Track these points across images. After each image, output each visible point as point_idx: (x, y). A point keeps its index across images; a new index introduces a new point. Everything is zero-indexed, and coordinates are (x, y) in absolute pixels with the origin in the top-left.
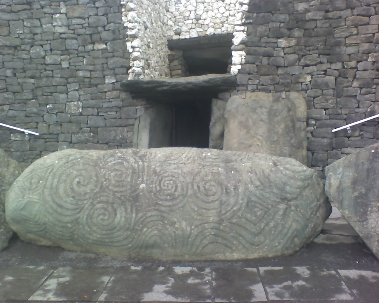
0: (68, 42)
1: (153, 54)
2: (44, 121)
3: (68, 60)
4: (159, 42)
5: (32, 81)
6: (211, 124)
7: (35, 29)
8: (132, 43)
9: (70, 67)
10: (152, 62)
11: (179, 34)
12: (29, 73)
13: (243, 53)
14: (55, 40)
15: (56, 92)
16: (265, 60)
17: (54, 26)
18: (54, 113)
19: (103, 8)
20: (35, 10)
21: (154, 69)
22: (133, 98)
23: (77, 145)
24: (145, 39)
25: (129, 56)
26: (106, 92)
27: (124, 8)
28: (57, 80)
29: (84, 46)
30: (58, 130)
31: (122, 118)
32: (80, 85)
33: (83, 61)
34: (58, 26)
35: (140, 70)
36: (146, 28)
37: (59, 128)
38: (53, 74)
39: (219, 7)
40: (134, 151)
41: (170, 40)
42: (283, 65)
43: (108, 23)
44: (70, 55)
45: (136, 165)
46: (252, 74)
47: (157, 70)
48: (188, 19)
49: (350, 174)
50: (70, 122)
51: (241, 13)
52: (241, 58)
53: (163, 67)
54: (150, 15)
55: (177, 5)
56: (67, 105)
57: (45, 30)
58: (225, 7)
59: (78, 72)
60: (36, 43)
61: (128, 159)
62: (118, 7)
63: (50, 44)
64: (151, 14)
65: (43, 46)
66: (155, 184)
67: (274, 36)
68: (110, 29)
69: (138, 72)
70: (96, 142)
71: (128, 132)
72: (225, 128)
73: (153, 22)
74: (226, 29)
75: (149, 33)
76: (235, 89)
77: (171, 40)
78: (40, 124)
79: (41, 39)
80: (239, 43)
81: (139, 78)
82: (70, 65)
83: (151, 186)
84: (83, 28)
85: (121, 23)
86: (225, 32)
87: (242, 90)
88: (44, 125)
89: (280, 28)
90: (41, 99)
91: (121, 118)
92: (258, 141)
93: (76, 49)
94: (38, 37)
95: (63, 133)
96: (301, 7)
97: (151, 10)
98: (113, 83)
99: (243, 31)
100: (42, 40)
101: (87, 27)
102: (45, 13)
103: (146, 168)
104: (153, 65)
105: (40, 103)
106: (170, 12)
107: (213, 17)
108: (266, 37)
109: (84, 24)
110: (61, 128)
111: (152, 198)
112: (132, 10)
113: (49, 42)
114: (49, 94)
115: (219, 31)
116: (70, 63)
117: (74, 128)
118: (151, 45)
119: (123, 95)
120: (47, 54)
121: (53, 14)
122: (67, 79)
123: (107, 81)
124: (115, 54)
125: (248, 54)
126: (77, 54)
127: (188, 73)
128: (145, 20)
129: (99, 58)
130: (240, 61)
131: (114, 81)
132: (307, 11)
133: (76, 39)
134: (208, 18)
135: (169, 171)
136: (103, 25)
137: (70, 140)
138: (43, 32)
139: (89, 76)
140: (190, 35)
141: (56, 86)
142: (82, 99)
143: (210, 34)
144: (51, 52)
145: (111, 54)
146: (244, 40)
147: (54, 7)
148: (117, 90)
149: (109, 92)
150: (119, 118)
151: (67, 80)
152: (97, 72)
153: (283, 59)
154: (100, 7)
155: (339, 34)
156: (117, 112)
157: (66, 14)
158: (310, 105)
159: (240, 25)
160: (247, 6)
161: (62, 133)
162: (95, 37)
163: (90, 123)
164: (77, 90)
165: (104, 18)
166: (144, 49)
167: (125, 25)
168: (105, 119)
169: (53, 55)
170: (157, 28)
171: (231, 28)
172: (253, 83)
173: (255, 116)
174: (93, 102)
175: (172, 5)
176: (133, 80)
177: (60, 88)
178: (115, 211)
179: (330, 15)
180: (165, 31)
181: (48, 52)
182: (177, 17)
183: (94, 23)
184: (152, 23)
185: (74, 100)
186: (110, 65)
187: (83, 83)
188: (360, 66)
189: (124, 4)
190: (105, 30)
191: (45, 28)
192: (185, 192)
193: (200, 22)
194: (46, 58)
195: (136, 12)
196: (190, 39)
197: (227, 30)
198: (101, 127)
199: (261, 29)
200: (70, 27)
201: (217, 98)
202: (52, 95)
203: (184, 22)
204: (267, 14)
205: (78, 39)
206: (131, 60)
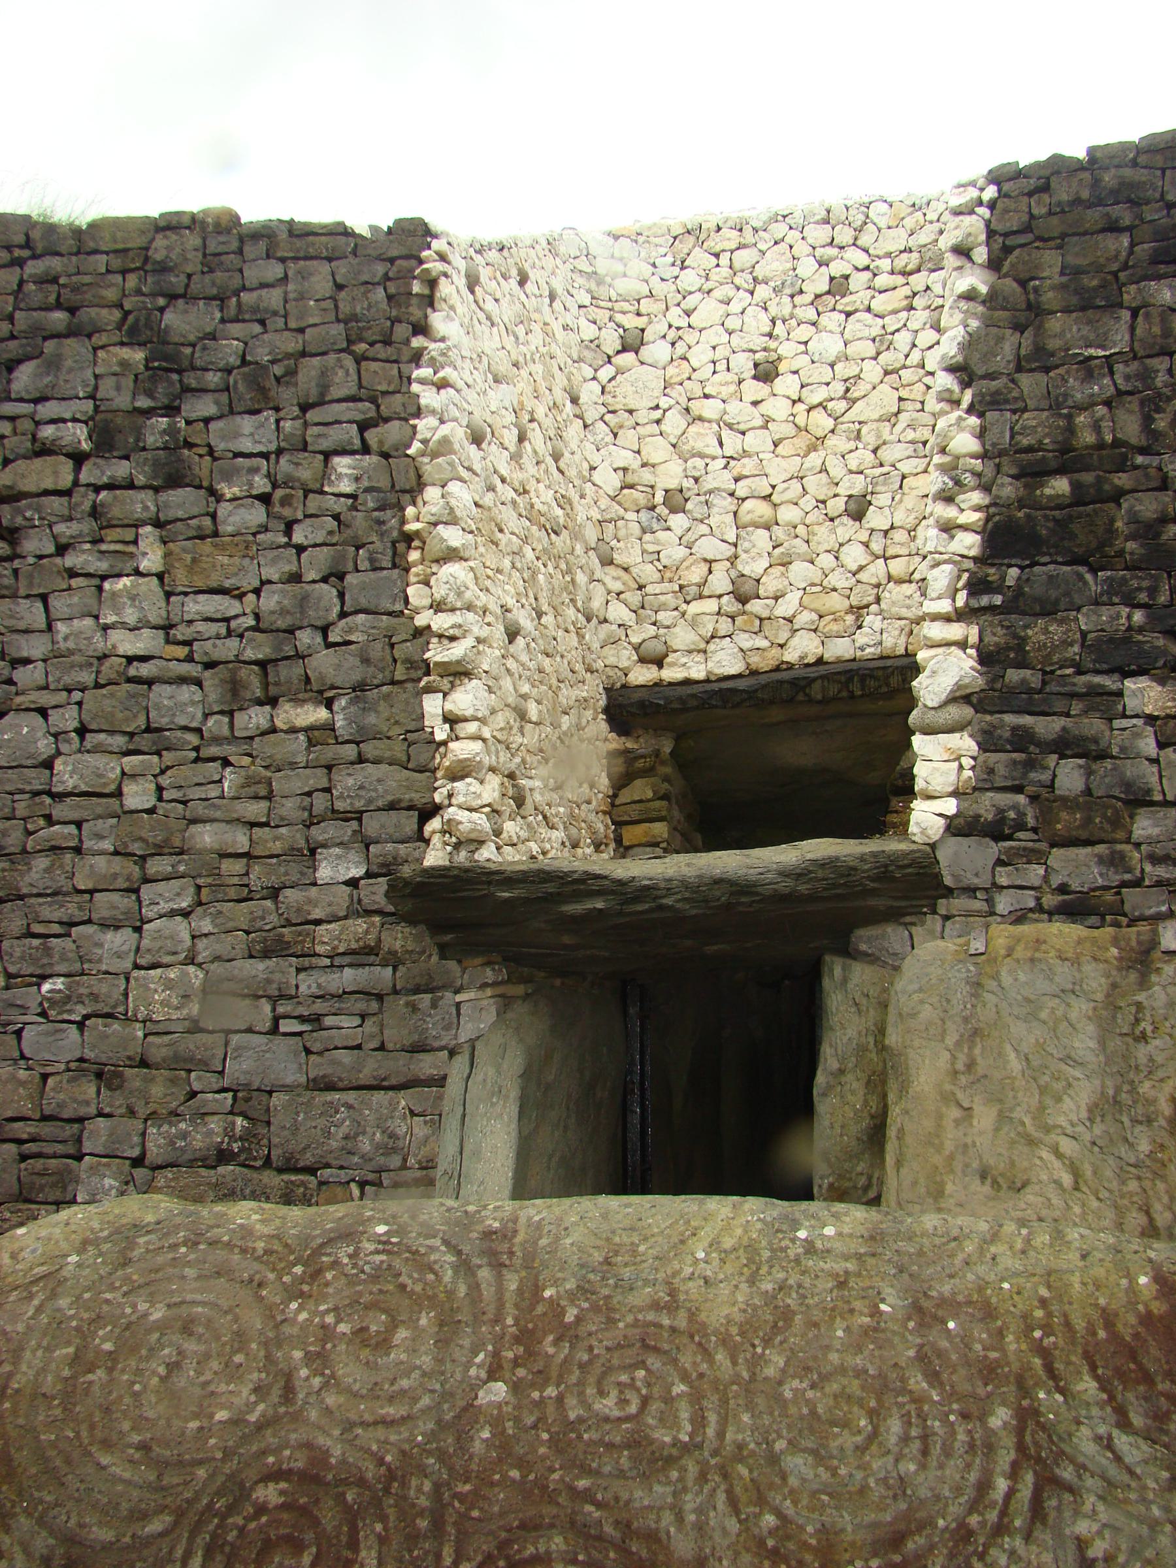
0: (162, 694)
1: (541, 751)
2: (23, 1057)
3: (155, 776)
4: (568, 695)
6: (821, 1079)
7: (21, 639)
8: (449, 697)
9: (162, 807)
10: (534, 785)
11: (659, 663)
13: (966, 743)
14: (103, 686)
15: (89, 921)
16: (1070, 777)
17: (106, 628)
18: (73, 1017)
19: (325, 549)
20: (31, 560)
21: (545, 817)
22: (444, 951)
23: (169, 1173)
24: (507, 683)
25: (434, 757)
26: (318, 922)
27: (416, 548)
29: (231, 714)
30: (88, 1103)
31: (390, 1046)
32: (199, 888)
33: (220, 781)
34: (123, 625)
35: (481, 820)
36: (512, 634)
37: (93, 1089)
38: (81, 841)
39: (841, 545)
40: (449, 1210)
41: (618, 685)
42: (1158, 797)
43: (343, 615)
44: (164, 753)
45: (462, 1290)
46: (1010, 838)
47: (556, 820)
48: (701, 597)
50: (144, 1063)
51: (947, 568)
52: (956, 764)
53: (584, 807)
54: (530, 580)
55: (647, 537)
56: (132, 981)
57: (62, 645)
58: (866, 545)
59: (195, 829)
60: (19, 700)
61: (422, 1250)
62: (394, 543)
63: (80, 704)
64: (534, 574)
65: (50, 712)
66: (558, 1386)
67: (1105, 666)
68: (353, 638)
69: (473, 830)
70: (259, 1163)
71: (413, 1114)
72: (891, 1097)
73: (545, 608)
74: (876, 637)
75: (524, 658)
76: (934, 912)
77: (624, 686)
79: (42, 682)
80: (943, 697)
81: (476, 856)
82: (160, 799)
83: (536, 1395)
84: (229, 633)
85: (401, 611)
86: (868, 650)
87: (969, 914)
88: (22, 1074)
89: (1130, 628)
91: (382, 1048)
92: (1057, 1164)
93: (194, 725)
95: (108, 1115)
97: (538, 558)
98: (353, 883)
99: (963, 645)
100: (46, 687)
101: (247, 629)
102: (72, 573)
103: (507, 1295)
104: (538, 797)
105: (12, 969)
106: (618, 566)
107: (813, 585)
108: (1069, 671)
109: (236, 617)
110: (99, 1092)
111: (544, 1458)
112: (452, 555)
113: (76, 696)
114: (56, 929)
115: (840, 649)
116: (160, 789)
118: (533, 710)
119: (398, 938)
120: (64, 748)
121: (104, 578)
122: (143, 858)
123: (324, 872)
124: (369, 749)
126: (197, 749)
127: (698, 839)
128: (511, 602)
129: (293, 765)
130: (953, 778)
131: (357, 872)
133: (199, 683)
134: (789, 593)
135: (630, 1318)
136: (319, 623)
137: (136, 1152)
138: (55, 655)
139: (246, 849)
140: (710, 664)
141: (91, 892)
142: (204, 950)
143: (802, 658)
144: (82, 738)
145: (350, 751)
146: (966, 686)
147: (113, 547)
148: (369, 913)
149: (329, 922)
150: (375, 1044)
151: (143, 868)
152: (283, 830)
153: (1155, 769)
154: (315, 546)
156: (363, 1017)
157: (160, 576)
159: (948, 619)
160: (978, 537)
161: (100, 1114)
163: (238, 1069)
164: (186, 914)
165: (328, 592)
166: (502, 725)
167: (420, 621)
168: (308, 1052)
169: (88, 752)
170: (561, 633)
171: (897, 633)
172: (1018, 882)
174: (259, 967)
175: (627, 536)
176: (444, 868)
178: (352, 1517)
180: (596, 645)
181: (68, 741)
182: (649, 589)
183: (283, 612)
184: (540, 615)
185: (167, 959)
186: (341, 796)
189: (417, 533)
190: (329, 645)
191: (66, 639)
192: (710, 1432)
193: (755, 606)
194: (59, 765)
195: (471, 563)
196: (707, 681)
197: (881, 643)
198: (286, 1088)
200: (172, 632)
202: (70, 935)
203: (684, 606)
204: (1065, 568)
205: (206, 684)
206: (439, 774)
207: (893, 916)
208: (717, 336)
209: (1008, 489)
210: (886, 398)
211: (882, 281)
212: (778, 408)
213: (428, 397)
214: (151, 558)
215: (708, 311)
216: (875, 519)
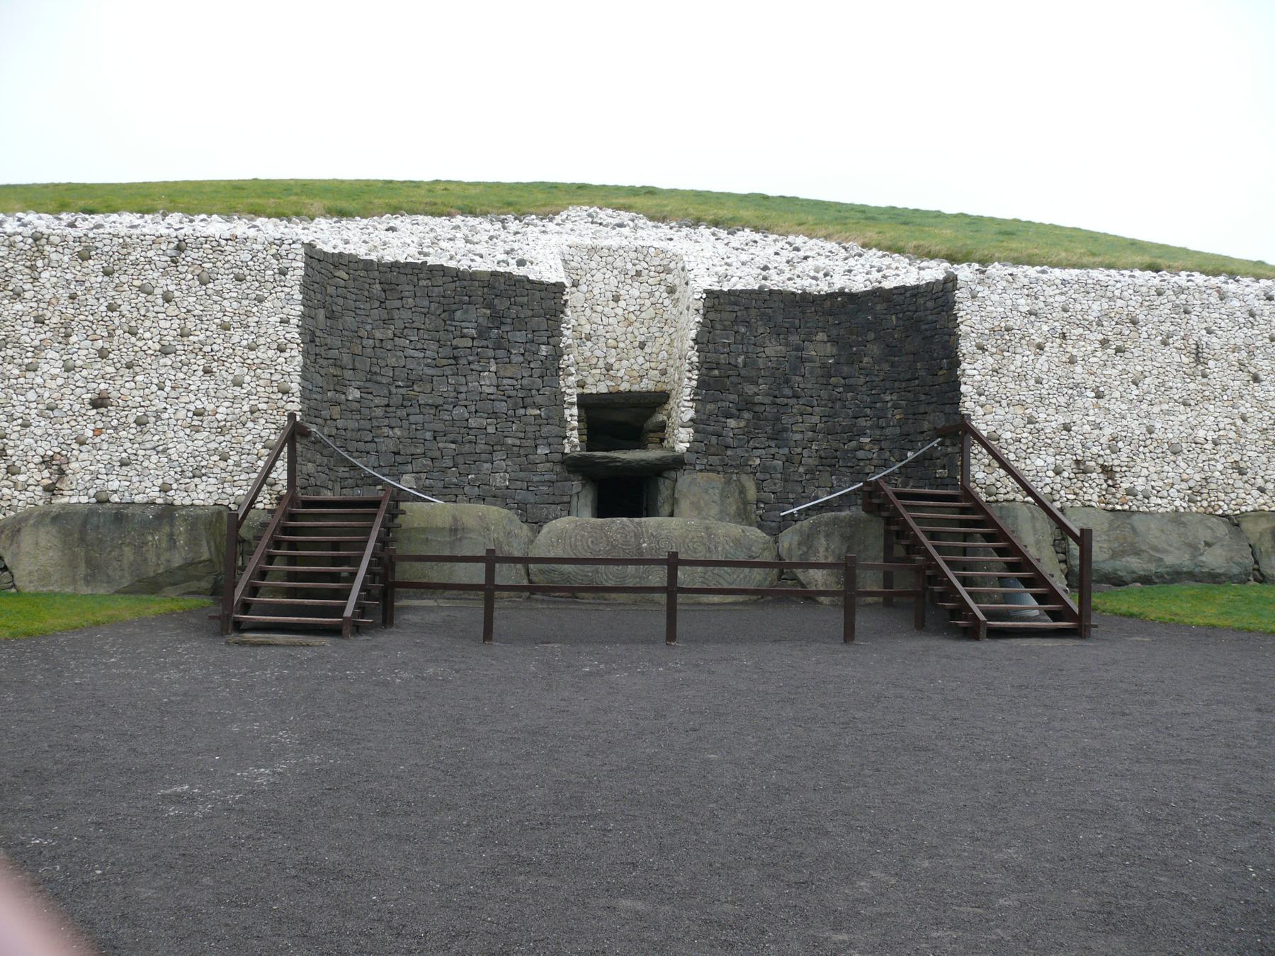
5: (453, 446)
12: (450, 437)
13: (691, 430)
16: (714, 440)
22: (569, 472)
28: (481, 447)
49: (796, 538)
78: (460, 497)
85: (558, 387)
94: (462, 396)
96: (750, 389)
115: (636, 388)
119: (558, 468)
123: (539, 451)
134: (621, 369)
155: (785, 420)
162: (528, 401)
165: (539, 380)
173: (707, 497)
174: (522, 474)
179: (778, 401)
187: (510, 453)
188: (806, 453)
199: (710, 407)
207: (674, 469)
209: (704, 371)
210: (651, 312)
211: (652, 274)
212: (620, 311)
213: (566, 332)
214: (493, 368)
215: (599, 276)
216: (647, 350)
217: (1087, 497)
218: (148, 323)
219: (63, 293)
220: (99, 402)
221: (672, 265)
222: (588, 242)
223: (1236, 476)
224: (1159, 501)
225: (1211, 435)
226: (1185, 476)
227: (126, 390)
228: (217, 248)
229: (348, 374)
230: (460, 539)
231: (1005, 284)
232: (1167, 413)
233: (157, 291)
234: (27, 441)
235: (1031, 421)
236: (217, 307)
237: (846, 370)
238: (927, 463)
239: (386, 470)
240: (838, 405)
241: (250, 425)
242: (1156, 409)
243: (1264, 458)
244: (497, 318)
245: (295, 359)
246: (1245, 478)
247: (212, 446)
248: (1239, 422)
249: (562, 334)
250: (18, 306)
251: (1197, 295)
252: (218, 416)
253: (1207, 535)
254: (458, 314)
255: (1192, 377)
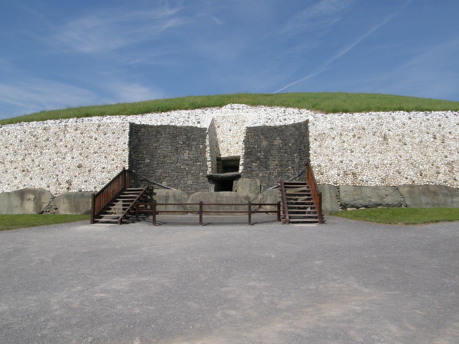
12: (176, 171)
16: (249, 169)
28: (185, 174)
90: (179, 180)
115: (236, 155)
117: (190, 189)
119: (206, 179)
125: (244, 167)
132: (261, 156)
134: (232, 150)
155: (269, 162)
158: (261, 182)
177: (185, 176)
187: (193, 175)
199: (248, 160)
201: (235, 180)
208: (226, 127)
210: (240, 134)
213: (207, 141)
215: (225, 124)
216: (239, 144)
217: (347, 182)
218: (91, 146)
219: (71, 139)
220: (80, 166)
221: (246, 120)
222: (223, 115)
223: (397, 174)
224: (371, 183)
225: (389, 162)
226: (380, 175)
227: (86, 163)
228: (108, 126)
229: (145, 156)
230: (168, 199)
231: (323, 120)
232: (374, 156)
233: (93, 137)
234: (63, 177)
235: (331, 160)
236: (108, 141)
237: (285, 148)
238: (304, 174)
239: (158, 181)
240: (283, 157)
241: (116, 170)
242: (370, 155)
243: (407, 168)
244: (188, 139)
245: (127, 152)
246: (400, 175)
247: (107, 176)
248: (399, 158)
249: (206, 142)
250: (61, 143)
251: (385, 120)
252: (108, 169)
253: (387, 193)
254: (177, 138)
255: (383, 144)
